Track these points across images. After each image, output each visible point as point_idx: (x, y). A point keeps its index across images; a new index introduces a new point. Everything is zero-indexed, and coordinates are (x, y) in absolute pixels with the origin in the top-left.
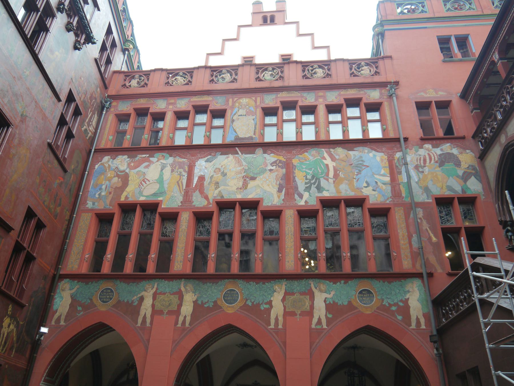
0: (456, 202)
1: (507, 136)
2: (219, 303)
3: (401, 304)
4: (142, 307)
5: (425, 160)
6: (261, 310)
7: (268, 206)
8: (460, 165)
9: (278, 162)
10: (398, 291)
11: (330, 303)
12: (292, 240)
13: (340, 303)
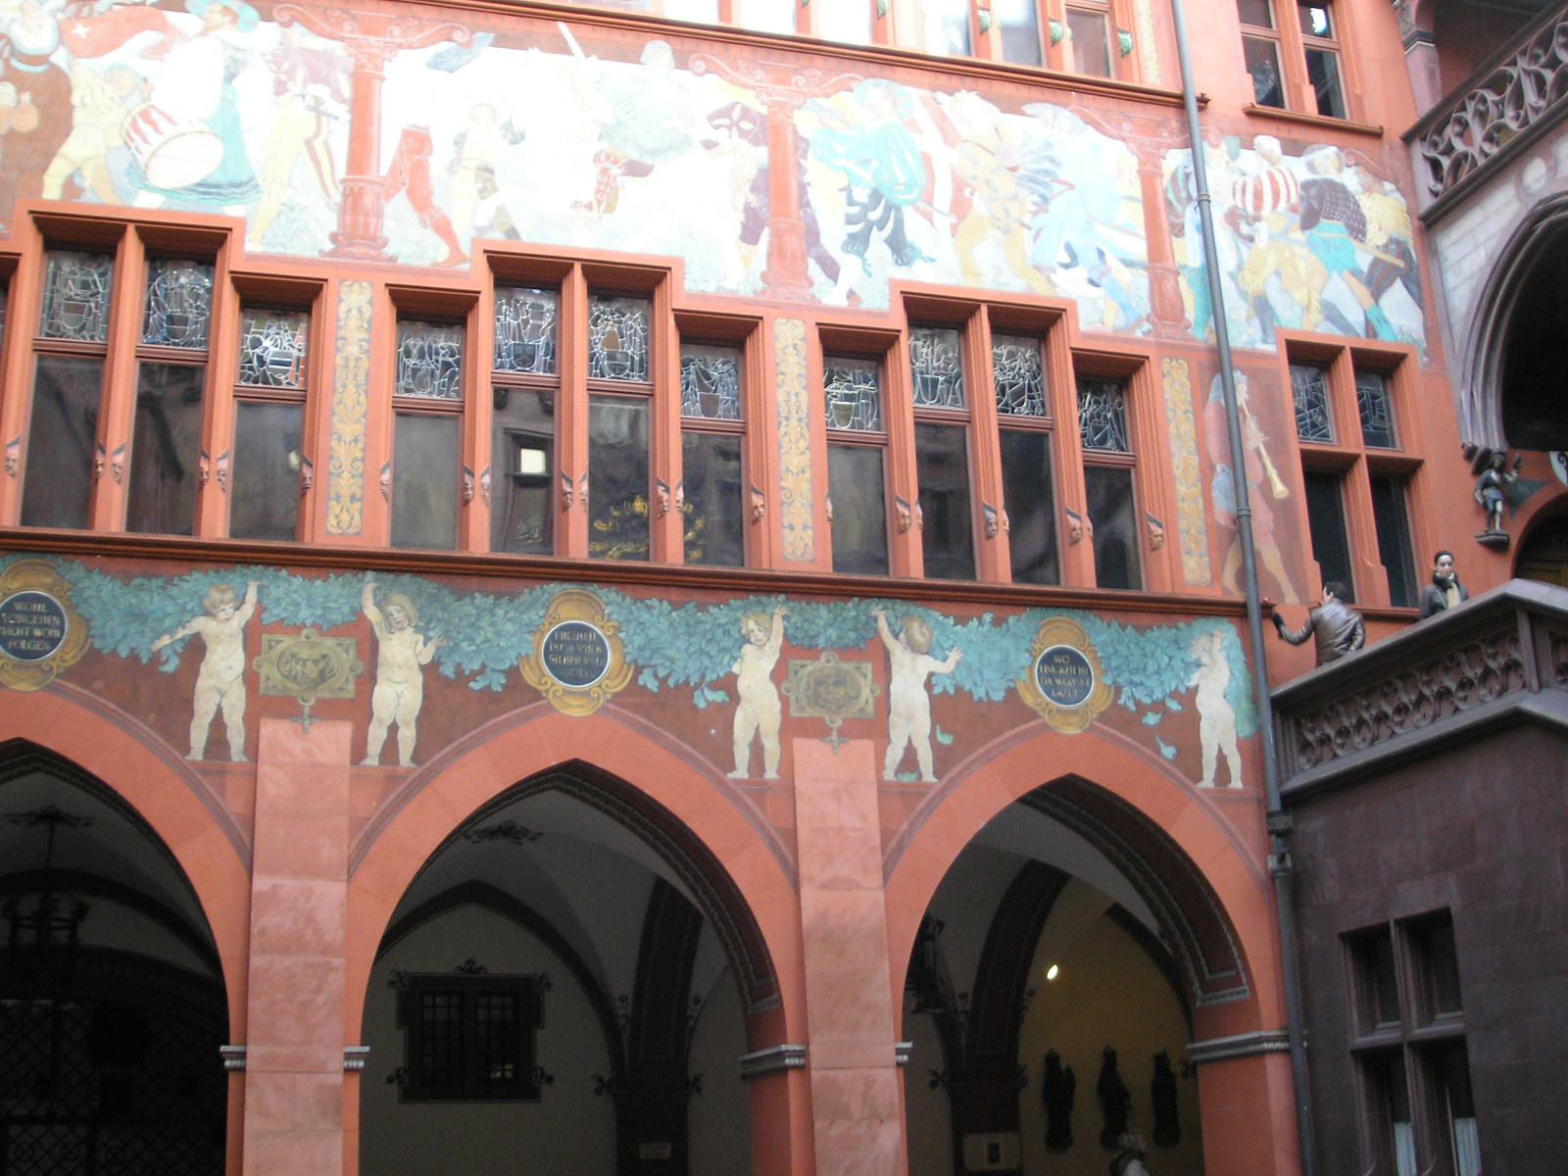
0: (1346, 366)
1: (1553, 169)
2: (530, 677)
3: (1174, 706)
4: (203, 683)
5: (1258, 196)
6: (694, 708)
7: (704, 296)
8: (1364, 235)
9: (736, 114)
10: (1166, 659)
11: (945, 692)
12: (803, 444)
13: (980, 693)
